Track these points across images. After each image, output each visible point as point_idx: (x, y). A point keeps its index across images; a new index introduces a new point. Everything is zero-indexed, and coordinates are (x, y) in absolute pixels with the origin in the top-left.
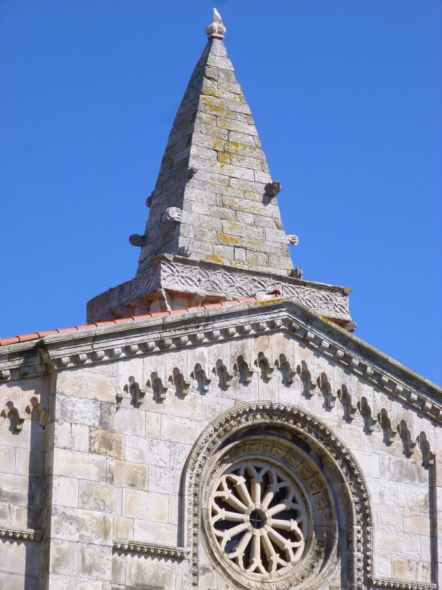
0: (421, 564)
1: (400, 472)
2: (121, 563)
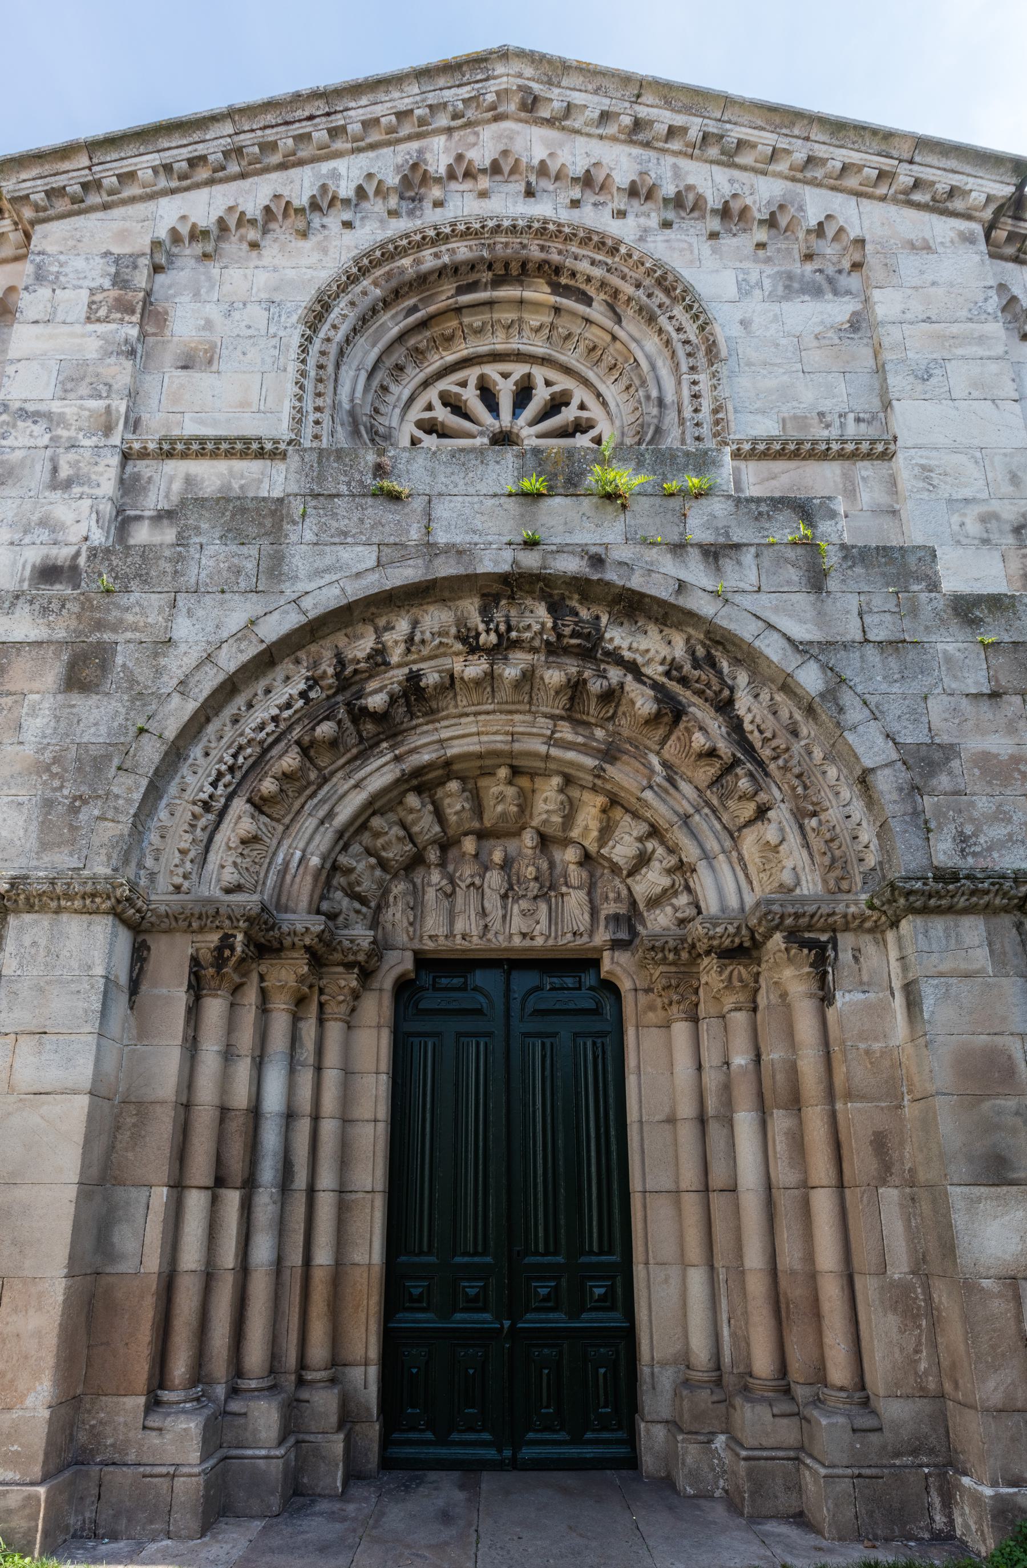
0: (851, 416)
1: (787, 287)
2: (150, 478)
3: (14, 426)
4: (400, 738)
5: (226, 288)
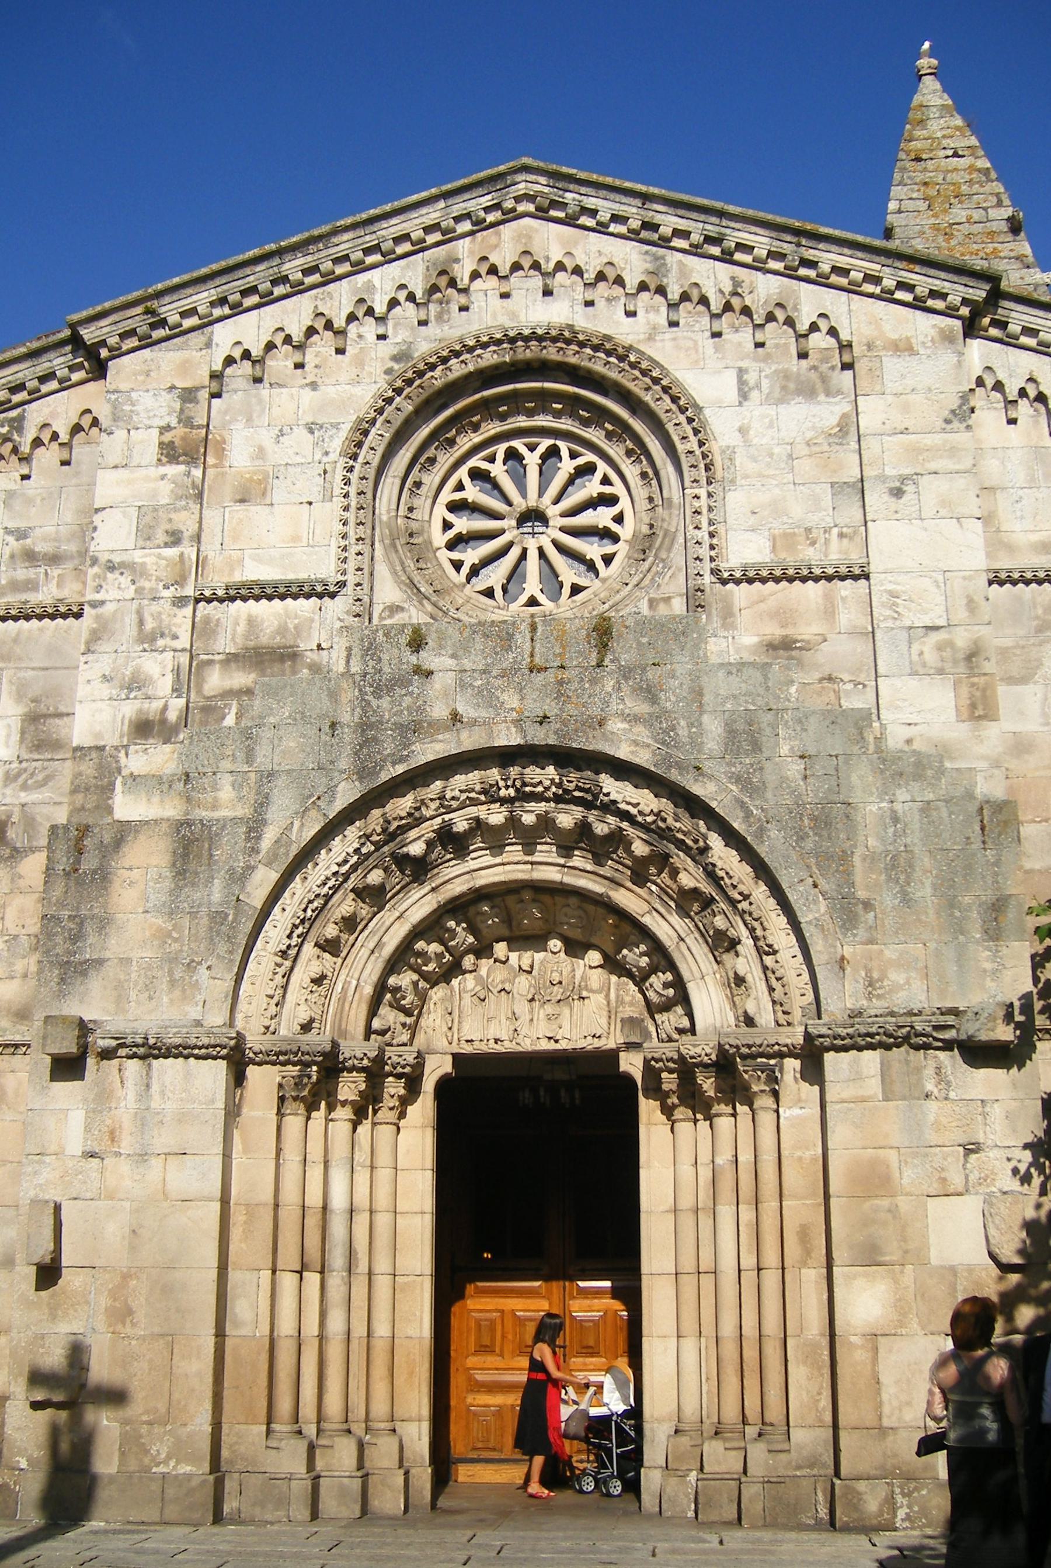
0: (835, 531)
1: (784, 388)
2: (218, 620)
3: (105, 579)
4: (436, 871)
5: (276, 411)
